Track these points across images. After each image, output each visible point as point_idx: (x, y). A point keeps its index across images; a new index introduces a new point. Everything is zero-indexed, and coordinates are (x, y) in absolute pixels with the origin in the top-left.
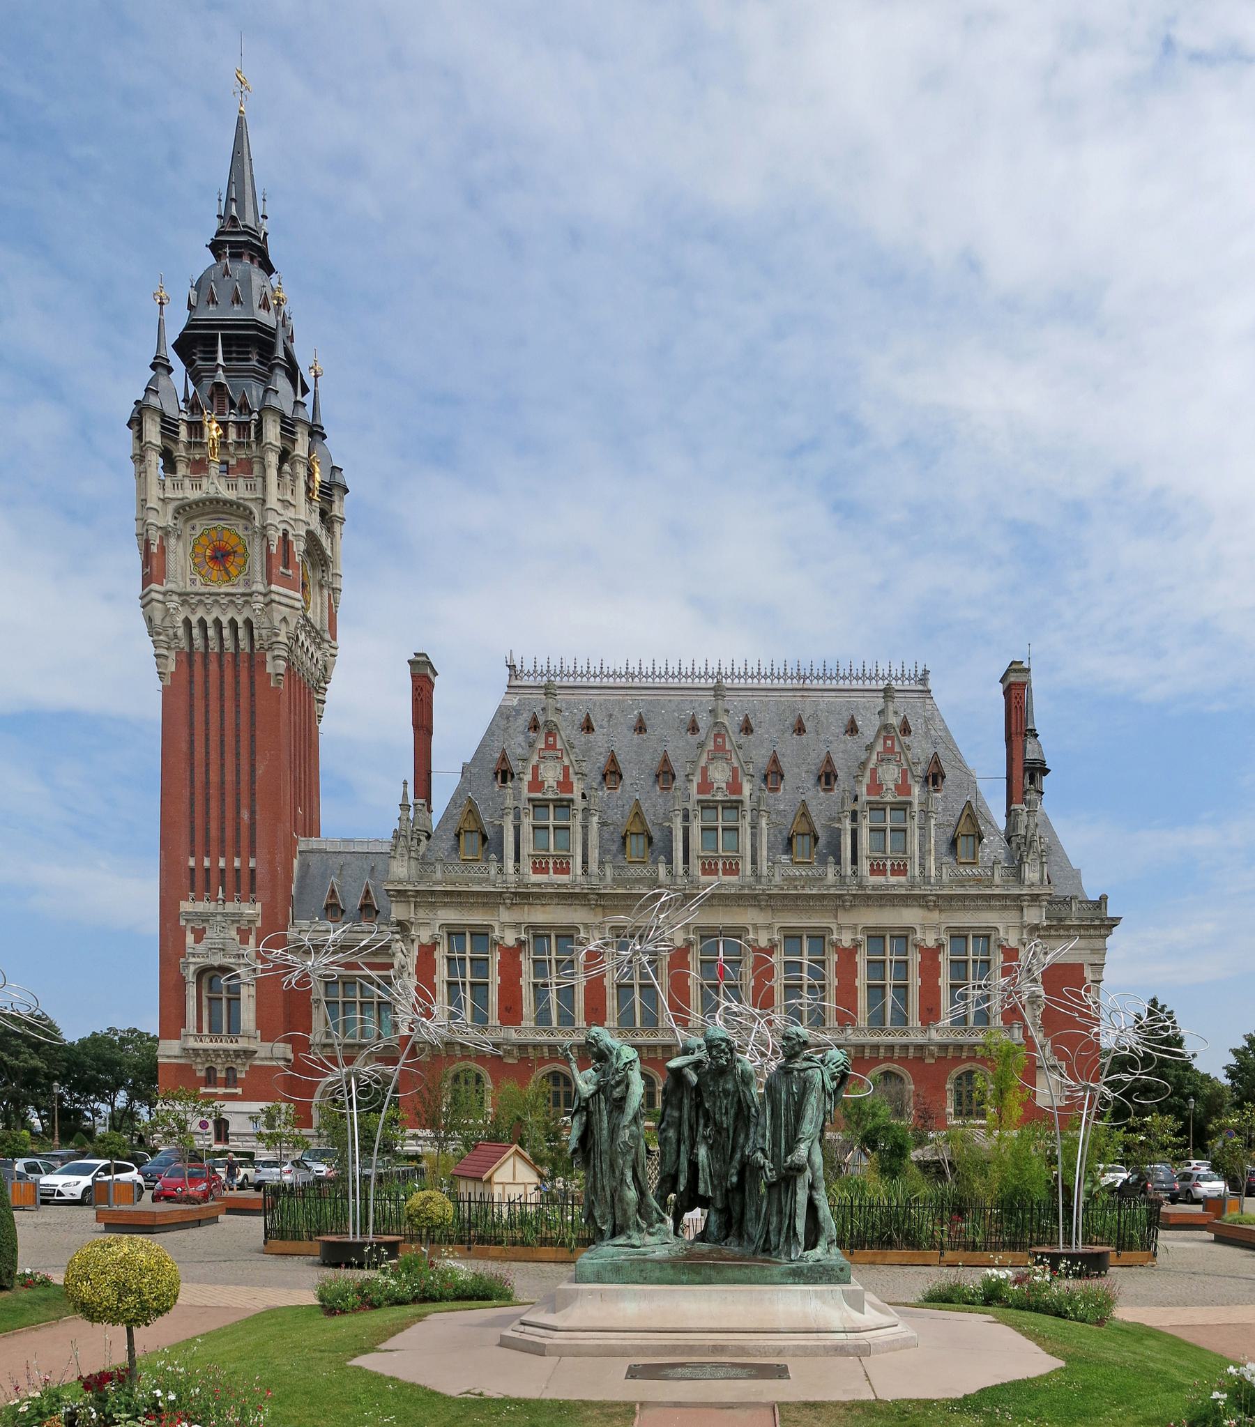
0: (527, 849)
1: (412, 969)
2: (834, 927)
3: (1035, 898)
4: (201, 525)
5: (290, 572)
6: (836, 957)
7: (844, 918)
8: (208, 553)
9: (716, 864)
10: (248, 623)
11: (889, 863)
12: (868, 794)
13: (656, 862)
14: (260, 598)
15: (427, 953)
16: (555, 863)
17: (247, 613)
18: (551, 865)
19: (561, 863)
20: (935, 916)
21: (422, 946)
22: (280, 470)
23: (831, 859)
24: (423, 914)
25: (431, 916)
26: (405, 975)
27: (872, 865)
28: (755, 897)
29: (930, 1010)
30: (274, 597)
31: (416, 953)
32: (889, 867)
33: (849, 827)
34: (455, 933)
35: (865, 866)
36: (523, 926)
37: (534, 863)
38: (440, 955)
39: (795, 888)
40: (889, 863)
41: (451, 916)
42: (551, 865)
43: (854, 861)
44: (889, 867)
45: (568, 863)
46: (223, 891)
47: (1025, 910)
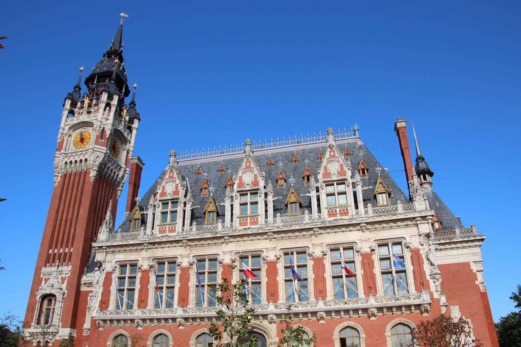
0: (157, 222)
1: (101, 284)
2: (310, 246)
3: (424, 218)
4: (78, 131)
5: (103, 141)
6: (312, 262)
7: (315, 240)
8: (79, 140)
9: (247, 220)
10: (86, 160)
11: (338, 210)
12: (324, 177)
13: (217, 222)
14: (90, 150)
15: (109, 275)
16: (169, 228)
17: (86, 157)
18: (167, 229)
19: (172, 227)
20: (367, 234)
21: (106, 273)
22: (105, 110)
23: (306, 211)
24: (109, 257)
25: (113, 258)
26: (98, 286)
27: (329, 212)
28: (266, 233)
29: (370, 288)
30: (95, 149)
31: (104, 276)
32: (338, 212)
33: (315, 195)
34: (123, 266)
35: (325, 212)
36: (152, 259)
37: (160, 229)
38: (115, 277)
39: (286, 226)
40: (338, 210)
41: (122, 257)
42: (167, 229)
43: (319, 211)
44: (338, 212)
45: (175, 227)
46: (59, 262)
47: (419, 225)
